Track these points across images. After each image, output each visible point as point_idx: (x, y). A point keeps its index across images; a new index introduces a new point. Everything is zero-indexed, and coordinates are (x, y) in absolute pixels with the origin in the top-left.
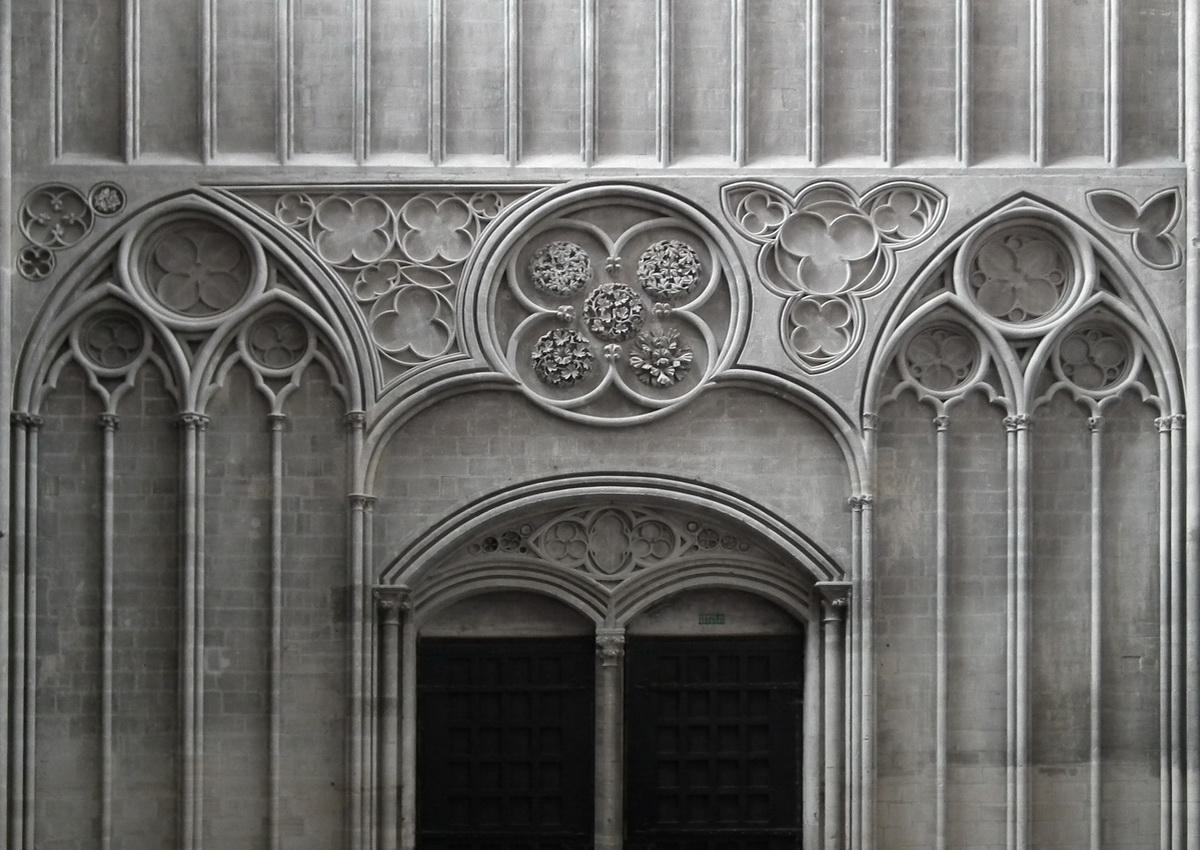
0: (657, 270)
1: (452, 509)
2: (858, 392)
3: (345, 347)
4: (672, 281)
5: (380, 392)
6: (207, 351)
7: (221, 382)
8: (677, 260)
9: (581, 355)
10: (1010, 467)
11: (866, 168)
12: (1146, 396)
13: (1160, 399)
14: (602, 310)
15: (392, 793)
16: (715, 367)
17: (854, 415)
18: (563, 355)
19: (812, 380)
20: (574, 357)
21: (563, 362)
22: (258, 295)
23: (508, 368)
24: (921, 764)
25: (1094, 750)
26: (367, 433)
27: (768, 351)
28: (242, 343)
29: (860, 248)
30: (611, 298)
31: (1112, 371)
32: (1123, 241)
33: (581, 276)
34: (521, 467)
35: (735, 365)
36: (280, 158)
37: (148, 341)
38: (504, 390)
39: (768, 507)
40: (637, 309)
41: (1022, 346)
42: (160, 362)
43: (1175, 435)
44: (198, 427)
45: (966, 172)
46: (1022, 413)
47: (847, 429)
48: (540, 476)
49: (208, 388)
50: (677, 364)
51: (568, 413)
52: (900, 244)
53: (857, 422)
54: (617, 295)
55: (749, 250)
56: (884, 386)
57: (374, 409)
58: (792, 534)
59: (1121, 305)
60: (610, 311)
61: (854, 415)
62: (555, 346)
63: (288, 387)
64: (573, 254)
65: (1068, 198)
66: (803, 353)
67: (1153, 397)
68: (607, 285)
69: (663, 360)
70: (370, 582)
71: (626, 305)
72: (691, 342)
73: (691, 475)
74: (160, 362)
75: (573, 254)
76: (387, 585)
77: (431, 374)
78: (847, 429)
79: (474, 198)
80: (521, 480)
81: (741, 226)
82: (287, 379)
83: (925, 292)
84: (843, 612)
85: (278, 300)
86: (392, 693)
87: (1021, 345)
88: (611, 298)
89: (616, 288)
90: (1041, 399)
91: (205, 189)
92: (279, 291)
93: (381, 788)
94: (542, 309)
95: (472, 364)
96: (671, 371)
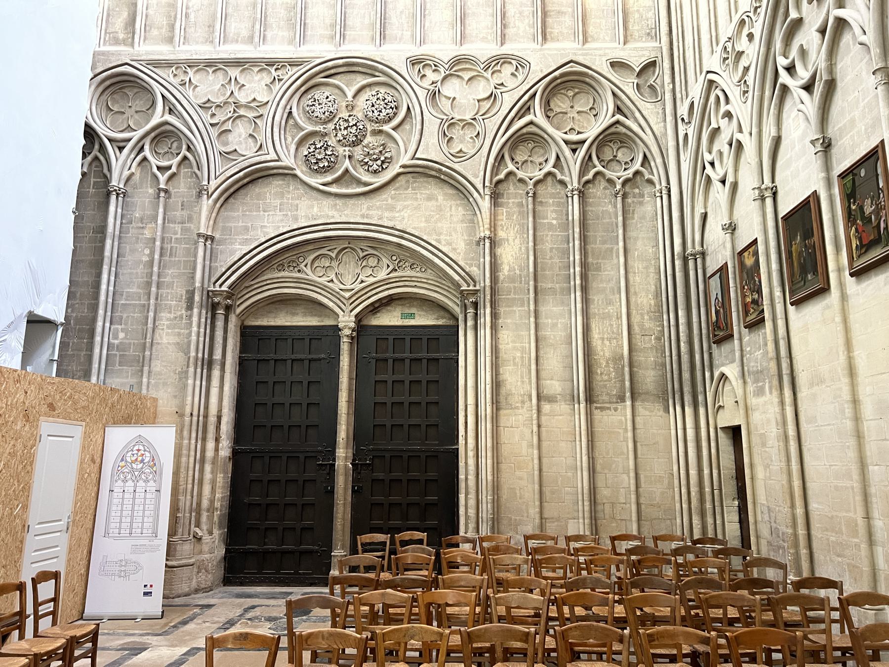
0: (373, 106)
1: (256, 244)
2: (482, 173)
3: (200, 148)
4: (380, 111)
5: (218, 174)
6: (126, 151)
7: (133, 170)
8: (384, 100)
9: (329, 153)
10: (570, 218)
11: (482, 48)
12: (647, 176)
13: (655, 179)
14: (342, 128)
15: (212, 419)
16: (405, 160)
17: (480, 186)
18: (320, 153)
19: (456, 167)
20: (326, 155)
21: (319, 157)
22: (155, 120)
23: (288, 160)
24: (523, 402)
25: (628, 394)
26: (209, 197)
27: (432, 150)
28: (147, 147)
29: (482, 89)
30: (347, 121)
31: (626, 163)
32: (628, 84)
33: (331, 109)
34: (296, 219)
35: (413, 158)
36: (174, 47)
37: (97, 147)
38: (287, 174)
39: (434, 243)
40: (361, 127)
41: (574, 146)
42: (102, 158)
43: (665, 197)
44: (118, 194)
45: (541, 50)
46: (576, 184)
47: (476, 195)
48: (306, 225)
49: (126, 173)
50: (382, 158)
51: (322, 187)
52: (504, 89)
53: (481, 191)
54: (350, 119)
55: (422, 94)
56: (496, 170)
57: (213, 184)
58: (447, 259)
59: (628, 123)
60: (346, 128)
61: (480, 186)
62: (316, 148)
63: (170, 172)
64: (327, 98)
65: (597, 63)
66: (451, 151)
67: (651, 177)
68: (345, 115)
69: (375, 156)
70: (206, 286)
71: (355, 125)
72: (391, 145)
73: (390, 224)
74: (102, 158)
75: (327, 98)
76: (218, 289)
77: (246, 163)
78: (476, 195)
79: (275, 67)
80: (295, 227)
81: (418, 80)
82: (170, 168)
83: (520, 115)
84: (476, 305)
85: (166, 123)
86: (218, 356)
87: (574, 147)
88: (347, 121)
89: (350, 116)
90: (586, 178)
91: (133, 63)
92: (168, 118)
93: (206, 416)
94: (310, 128)
95: (268, 158)
96: (379, 162)
